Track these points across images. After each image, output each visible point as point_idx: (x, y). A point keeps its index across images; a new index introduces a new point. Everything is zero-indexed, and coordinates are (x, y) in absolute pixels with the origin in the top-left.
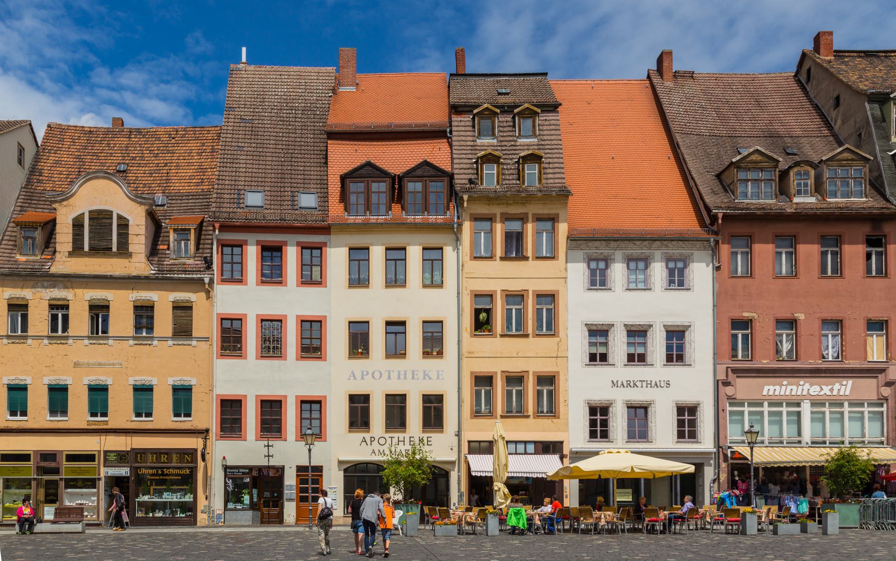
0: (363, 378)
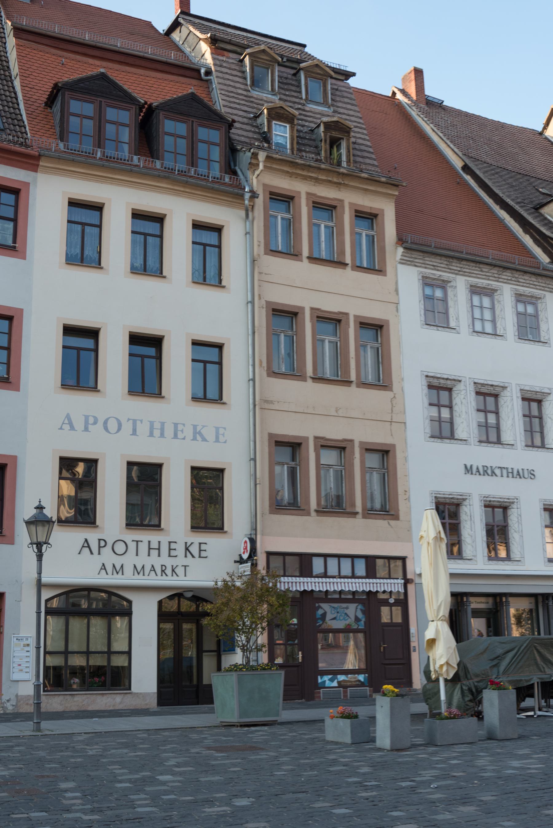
0: (86, 429)
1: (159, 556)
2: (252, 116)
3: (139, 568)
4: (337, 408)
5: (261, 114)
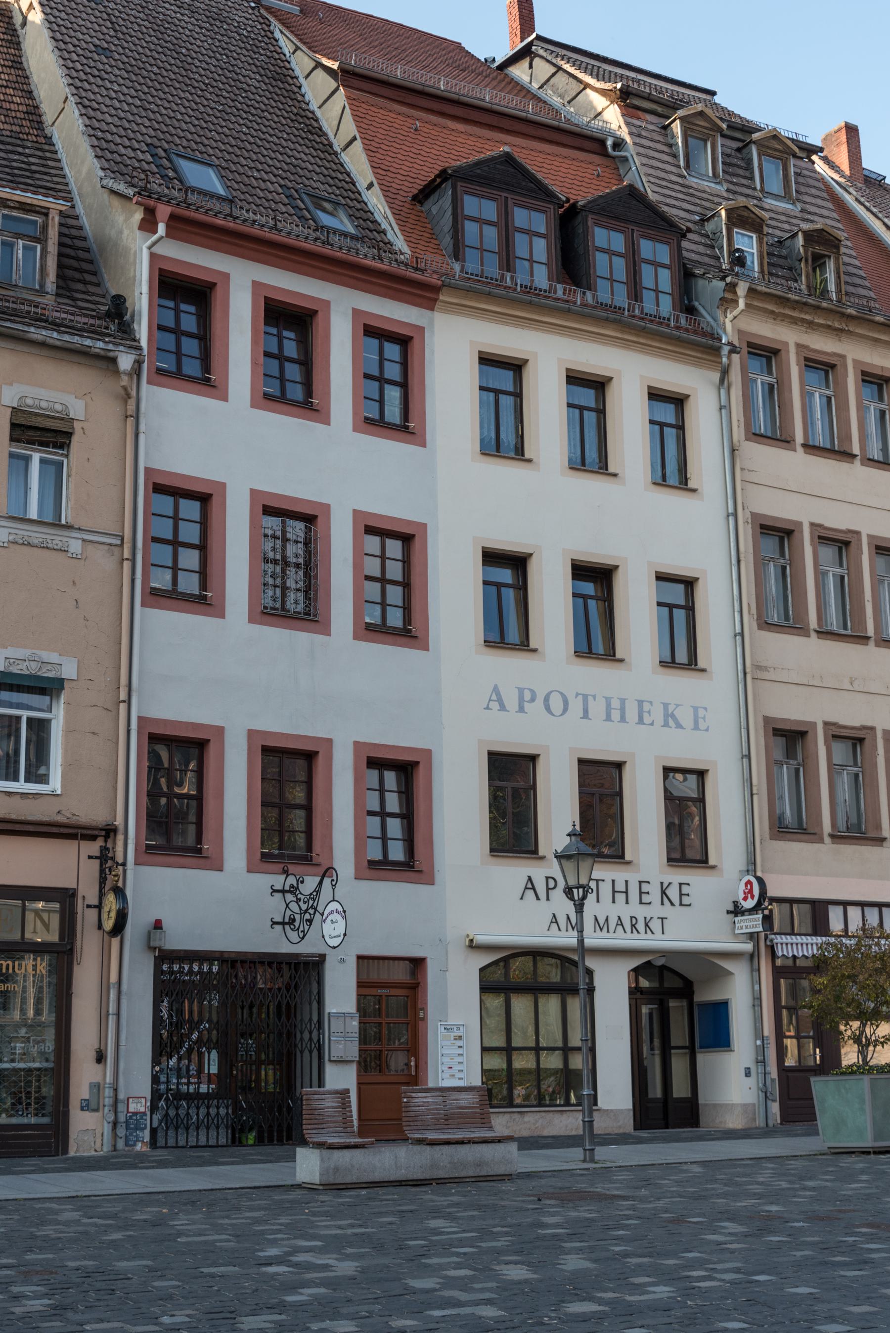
0: (521, 709)
1: (627, 902)
2: (698, 218)
3: (602, 921)
4: (851, 678)
5: (713, 216)
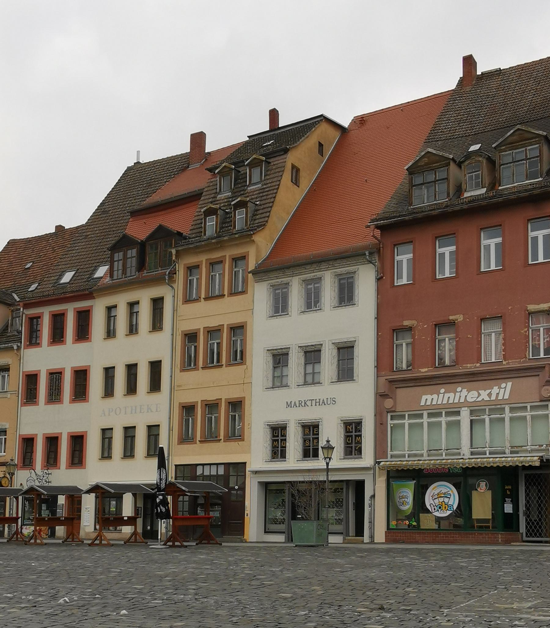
0: (109, 415)
